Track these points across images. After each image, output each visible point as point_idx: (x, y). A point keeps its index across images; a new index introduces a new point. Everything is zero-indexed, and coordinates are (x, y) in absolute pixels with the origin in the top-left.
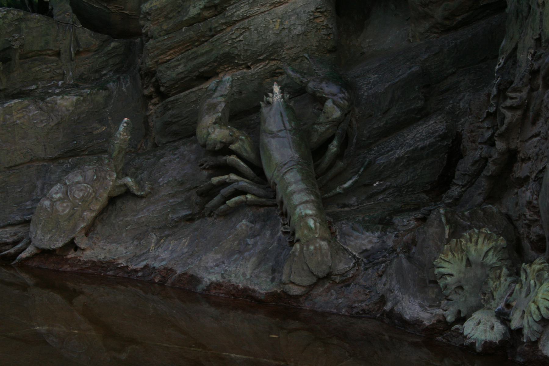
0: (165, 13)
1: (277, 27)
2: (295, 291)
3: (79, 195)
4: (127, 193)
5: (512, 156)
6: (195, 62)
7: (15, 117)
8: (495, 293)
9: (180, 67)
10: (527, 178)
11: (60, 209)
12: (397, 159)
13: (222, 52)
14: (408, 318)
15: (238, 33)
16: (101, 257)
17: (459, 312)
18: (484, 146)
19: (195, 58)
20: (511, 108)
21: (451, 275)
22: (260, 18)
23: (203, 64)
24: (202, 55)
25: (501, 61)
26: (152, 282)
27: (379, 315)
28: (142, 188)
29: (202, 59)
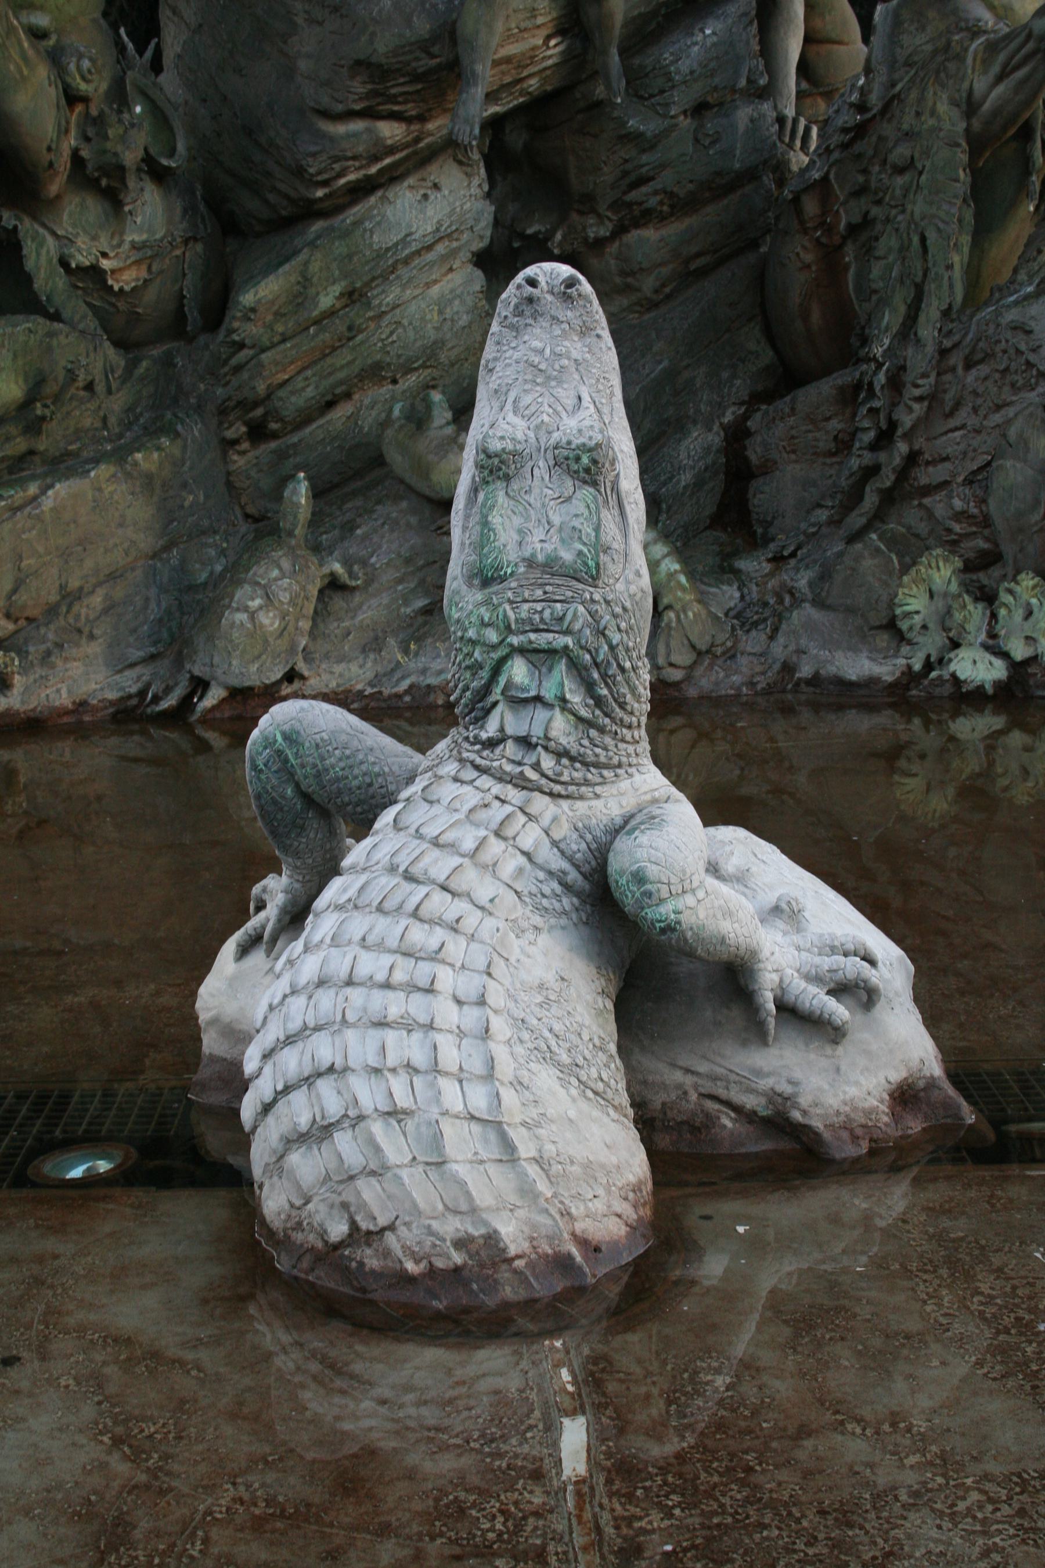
0: (276, 308)
1: (436, 318)
2: (676, 675)
3: (285, 597)
4: (334, 585)
5: (912, 459)
6: (331, 380)
7: (106, 492)
8: (967, 627)
9: (309, 389)
10: (945, 484)
11: (266, 621)
12: (685, 487)
13: (370, 361)
14: (854, 678)
15: (388, 331)
16: (333, 684)
17: (929, 656)
18: (865, 452)
19: (330, 374)
20: (920, 399)
21: (917, 612)
22: (413, 308)
23: (341, 382)
24: (342, 367)
25: (887, 342)
26: (434, 707)
27: (790, 686)
28: (351, 575)
29: (341, 375)
